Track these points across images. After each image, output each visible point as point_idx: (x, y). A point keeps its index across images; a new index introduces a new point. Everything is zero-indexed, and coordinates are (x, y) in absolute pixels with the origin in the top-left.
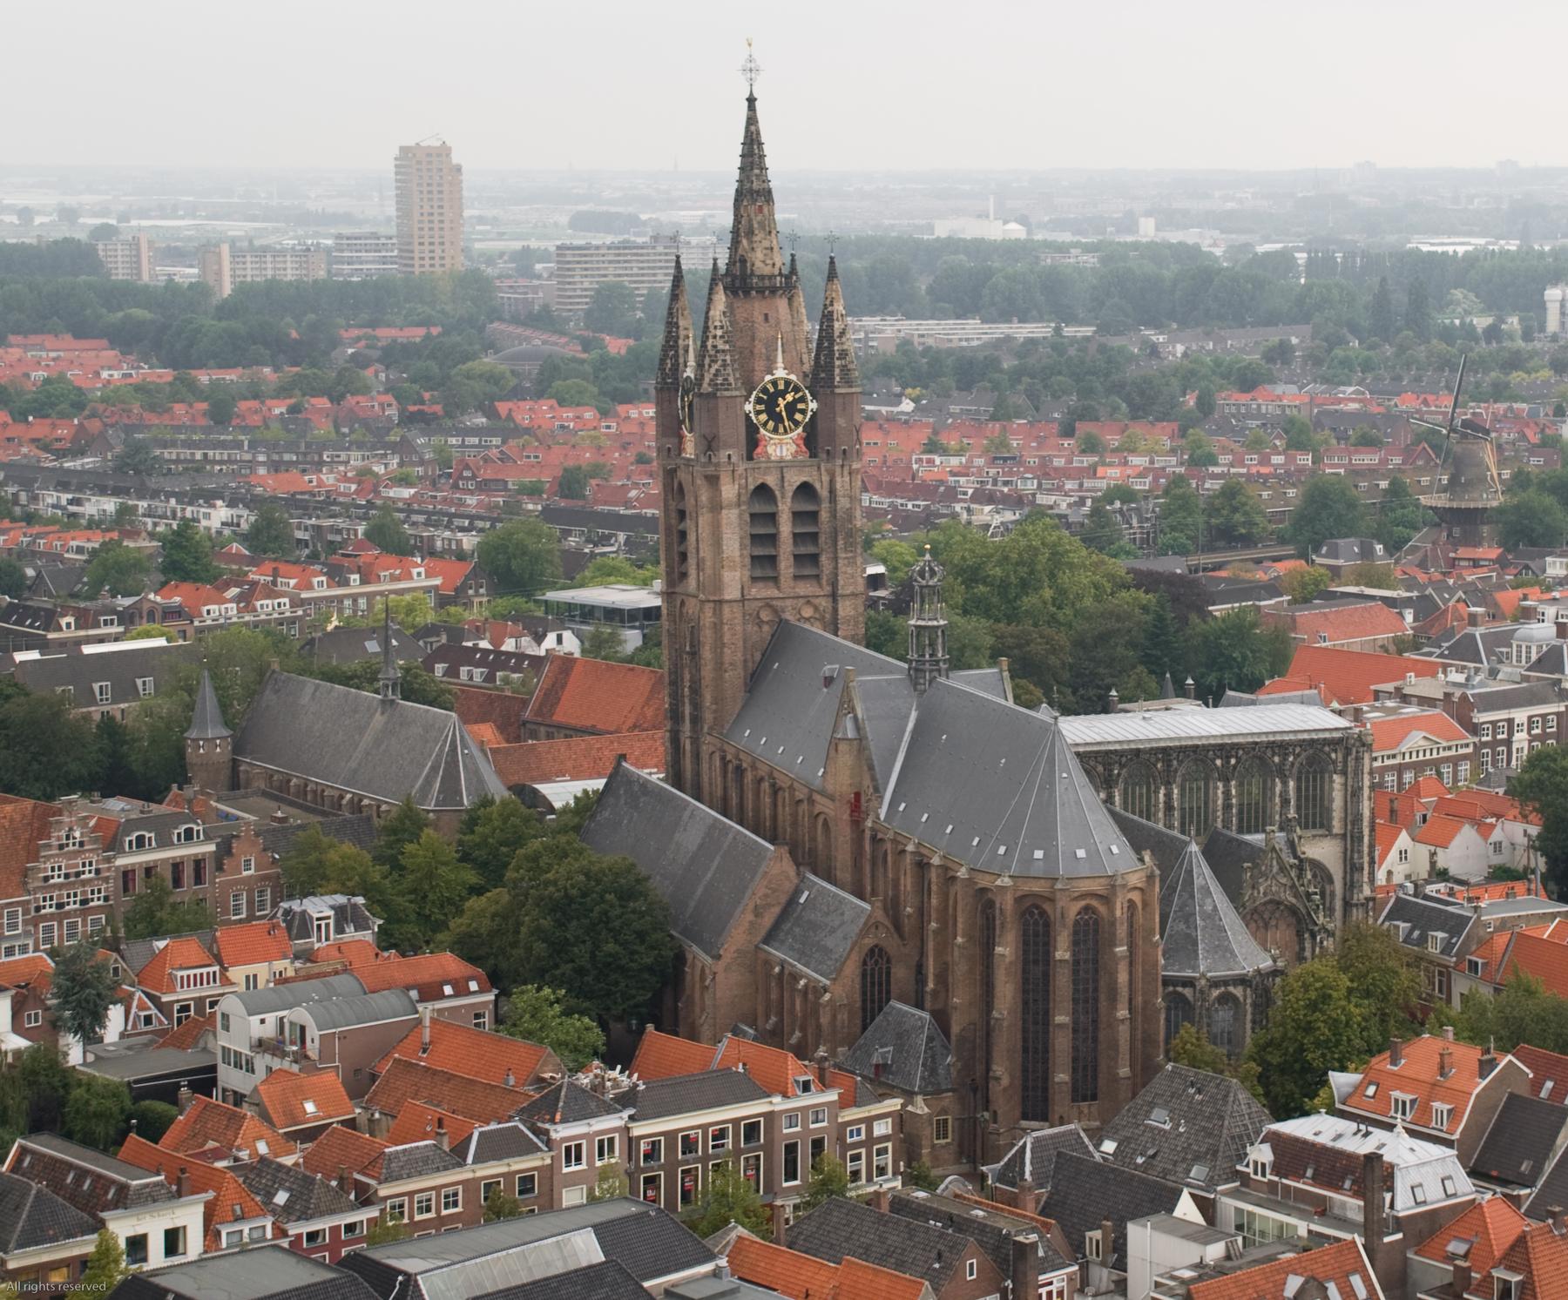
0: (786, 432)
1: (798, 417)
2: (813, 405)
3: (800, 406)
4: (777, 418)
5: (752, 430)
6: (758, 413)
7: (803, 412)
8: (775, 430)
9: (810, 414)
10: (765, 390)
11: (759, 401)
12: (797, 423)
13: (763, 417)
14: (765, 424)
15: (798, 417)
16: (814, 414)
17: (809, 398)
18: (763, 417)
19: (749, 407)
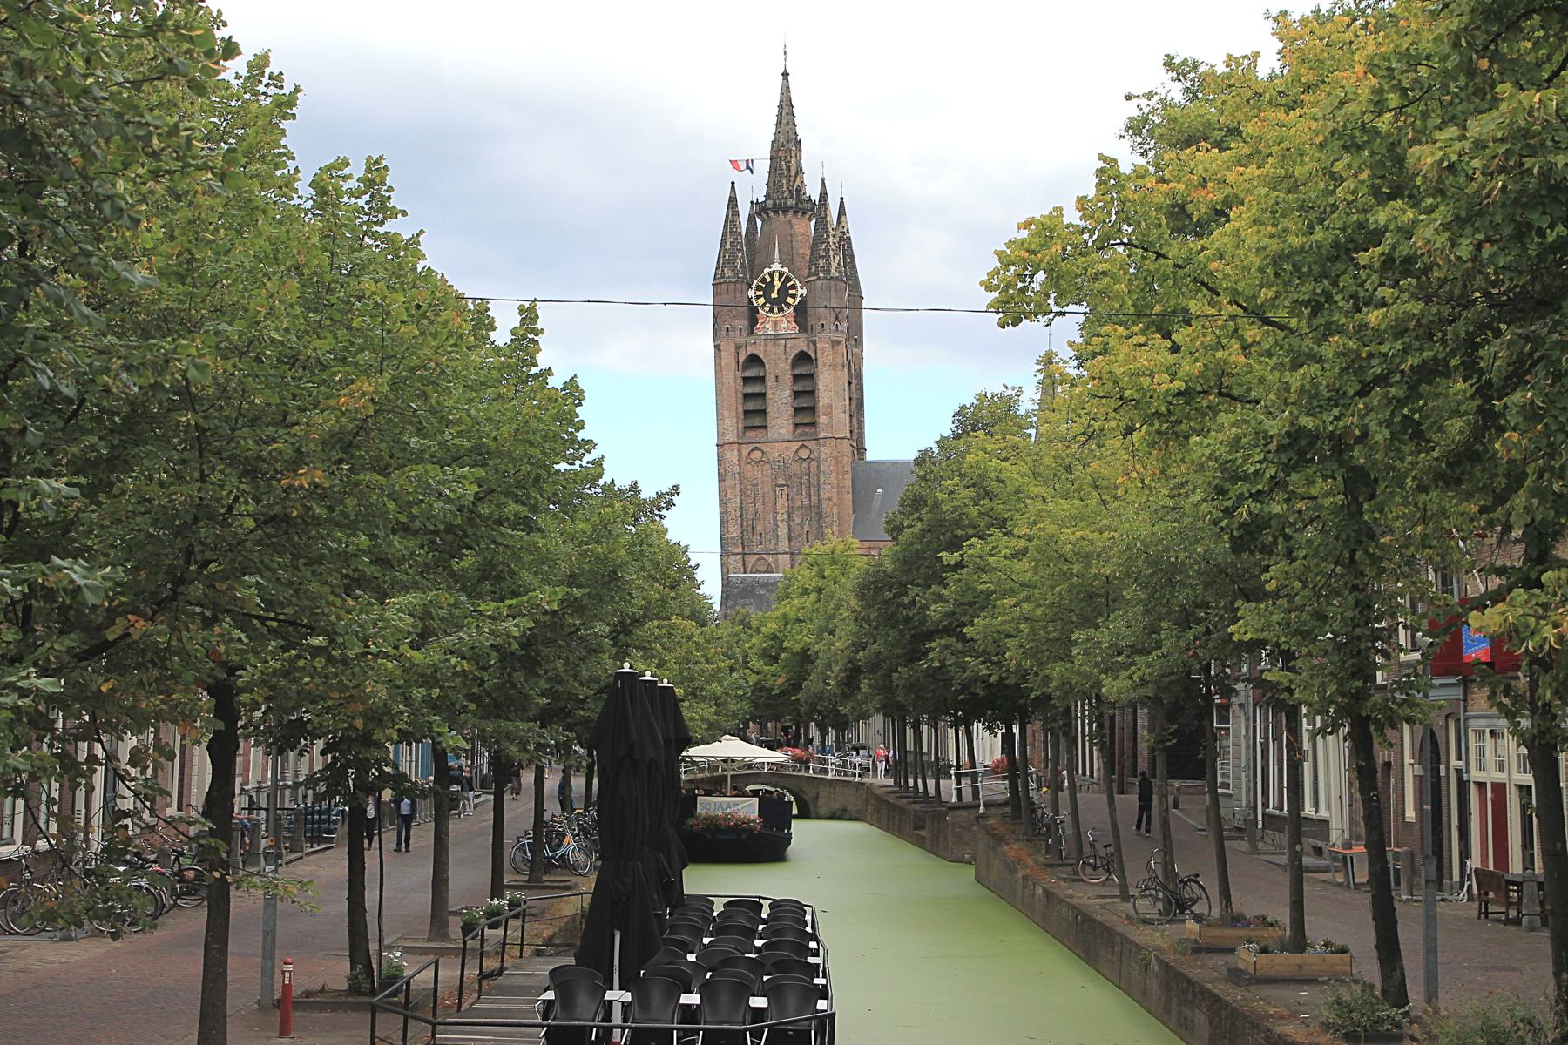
0: (781, 309)
1: (790, 300)
2: (804, 292)
3: (791, 292)
4: (774, 302)
5: (753, 311)
6: (758, 297)
7: (794, 296)
8: (771, 311)
9: (798, 299)
10: (763, 280)
11: (758, 288)
12: (788, 305)
13: (762, 301)
14: (763, 306)
15: (790, 300)
16: (803, 300)
17: (798, 285)
18: (762, 301)
19: (751, 293)
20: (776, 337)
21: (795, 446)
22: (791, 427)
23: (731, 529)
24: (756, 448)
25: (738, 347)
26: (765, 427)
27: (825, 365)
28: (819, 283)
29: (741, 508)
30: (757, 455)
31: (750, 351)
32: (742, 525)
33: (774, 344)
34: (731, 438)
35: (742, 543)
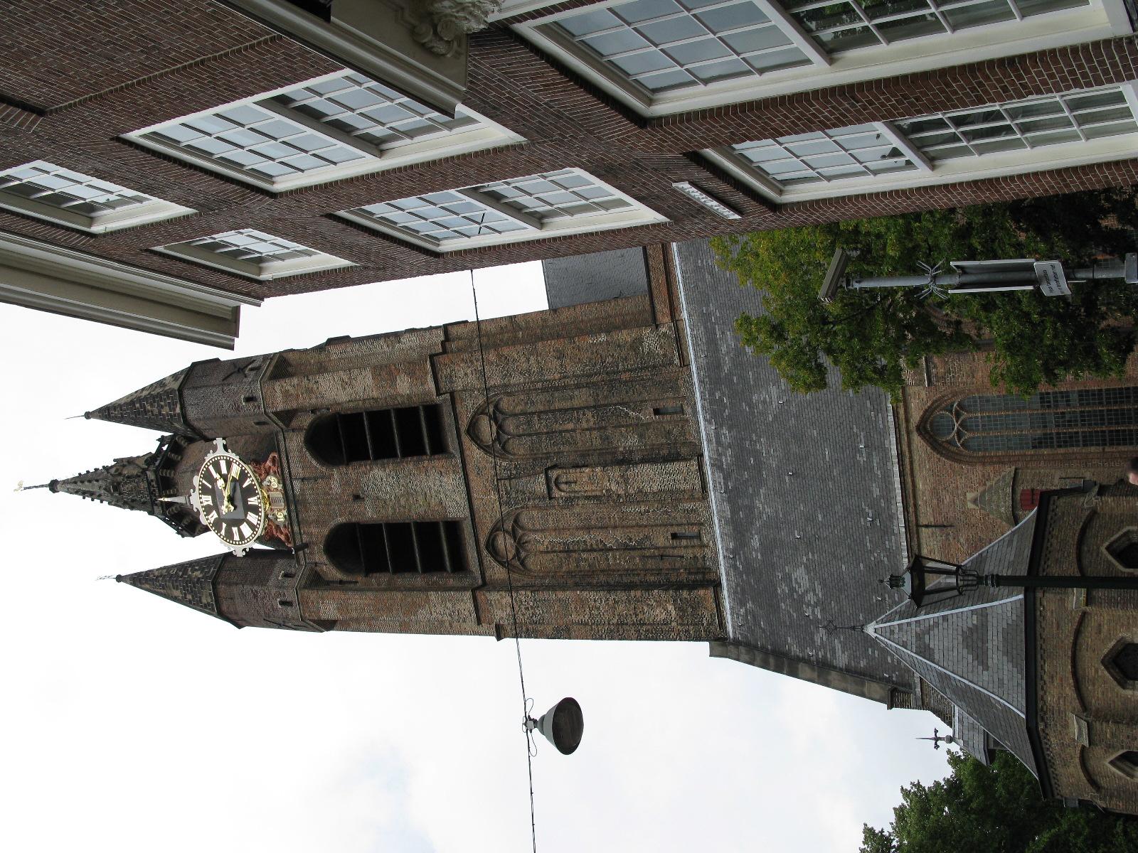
17: (210, 456)
20: (290, 500)
21: (474, 453)
22: (439, 463)
23: (659, 614)
24: (491, 546)
25: (316, 581)
26: (453, 527)
27: (310, 391)
28: (192, 413)
29: (610, 588)
30: (505, 543)
31: (320, 557)
32: (649, 587)
33: (305, 502)
34: (465, 603)
35: (692, 586)
